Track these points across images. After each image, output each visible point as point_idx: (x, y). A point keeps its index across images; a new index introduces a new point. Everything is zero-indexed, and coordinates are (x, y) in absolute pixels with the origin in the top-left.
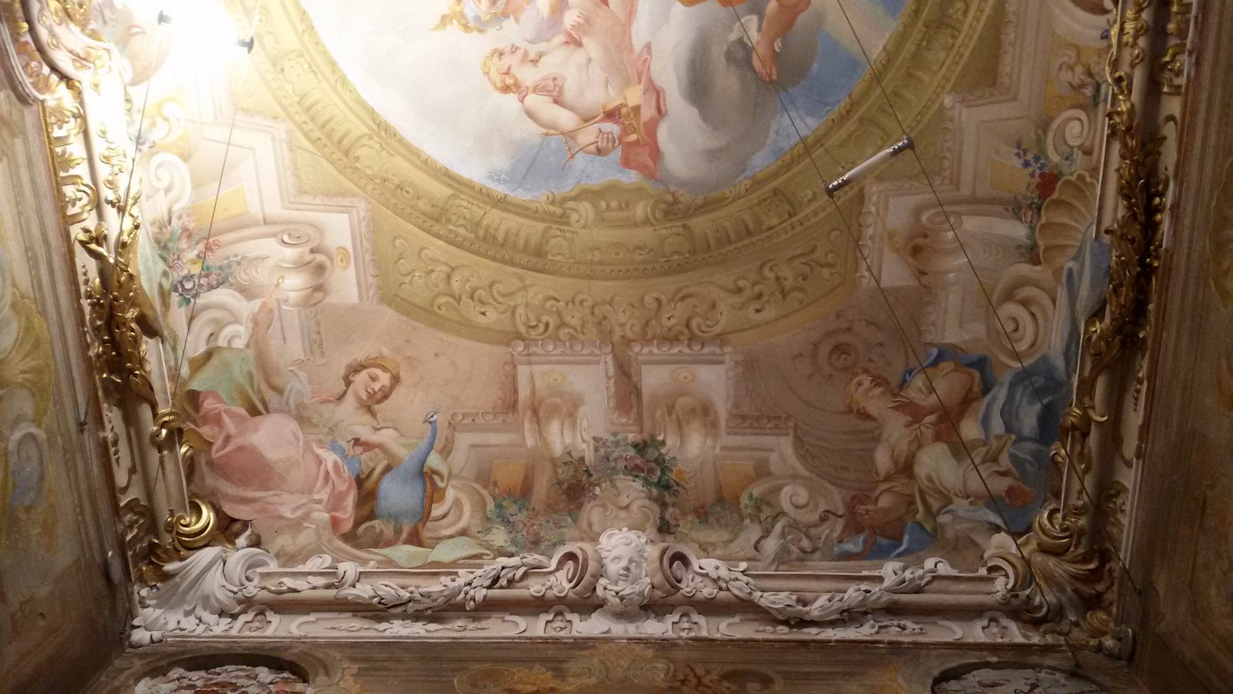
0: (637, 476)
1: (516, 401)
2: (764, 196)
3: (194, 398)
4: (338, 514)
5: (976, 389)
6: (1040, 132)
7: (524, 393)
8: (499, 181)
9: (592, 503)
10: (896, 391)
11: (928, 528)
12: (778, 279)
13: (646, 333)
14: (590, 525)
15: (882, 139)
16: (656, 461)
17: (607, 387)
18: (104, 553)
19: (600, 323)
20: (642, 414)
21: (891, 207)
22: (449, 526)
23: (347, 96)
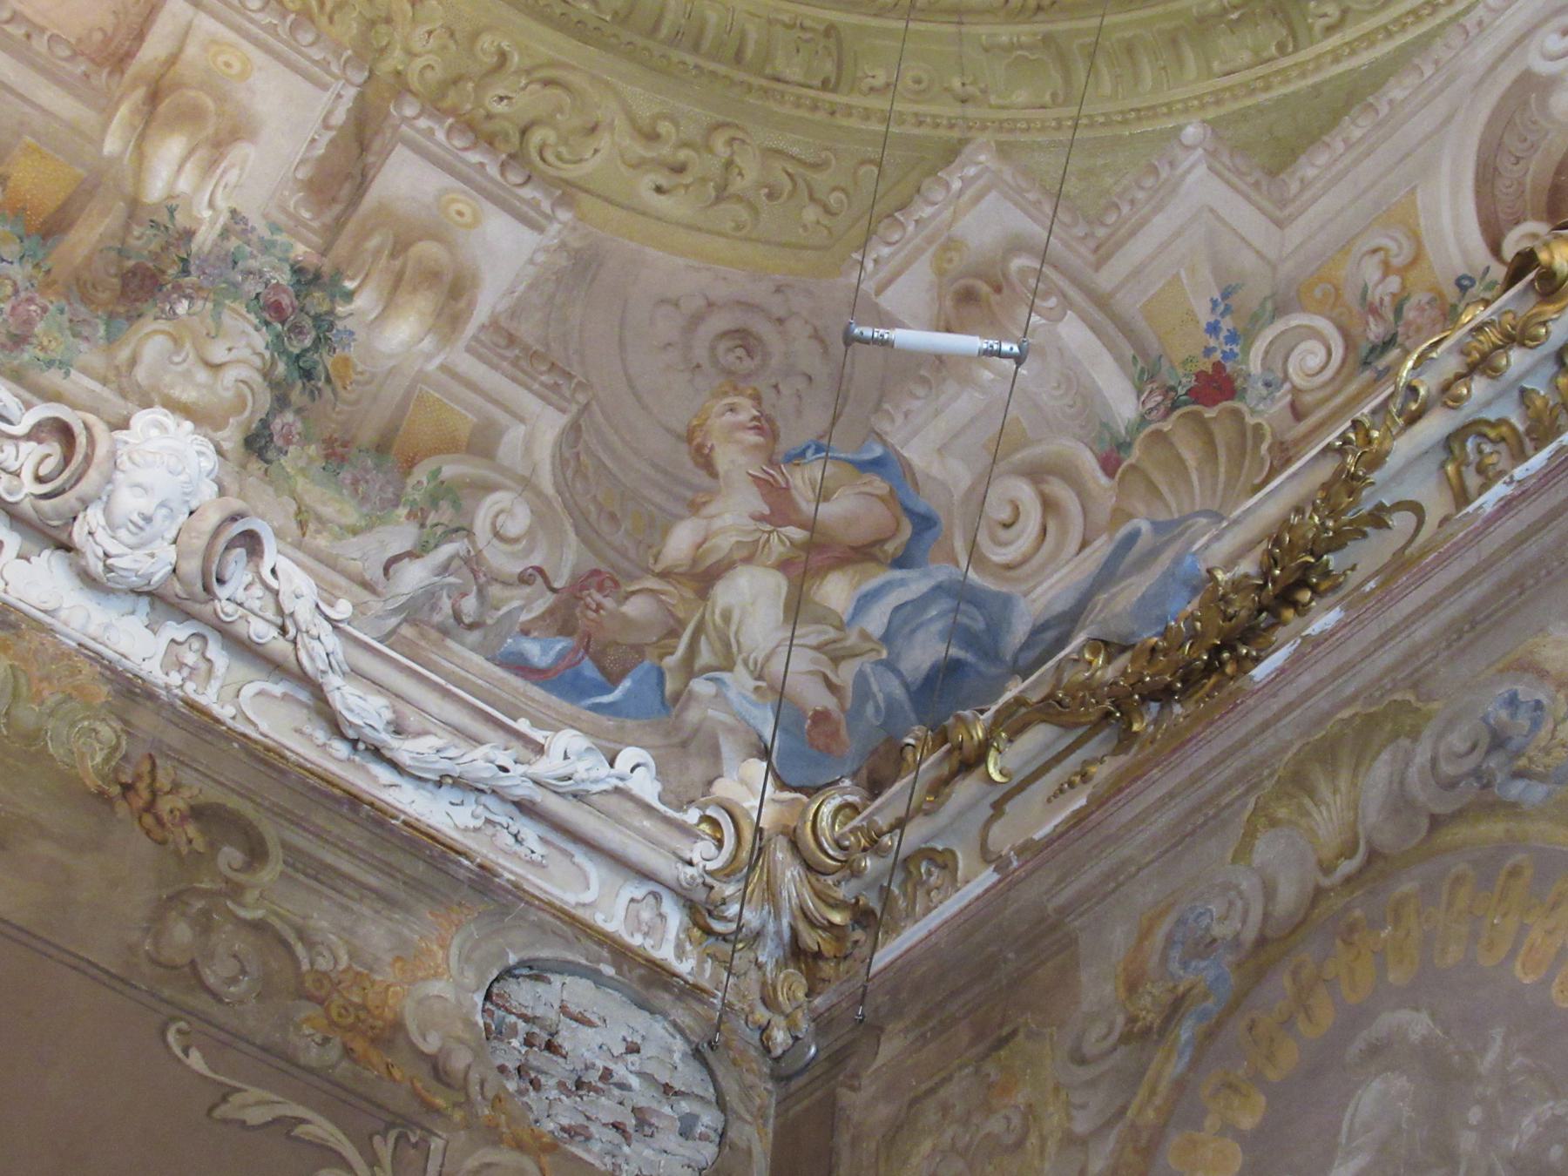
0: (267, 324)
1: (129, 55)
2: (808, 23)
6: (1269, 306)
7: (154, 49)
9: (162, 325)
10: (780, 458)
11: (670, 687)
12: (729, 164)
13: (444, 96)
14: (133, 362)
15: (1054, 95)
16: (317, 318)
17: (313, 140)
19: (372, 23)
20: (344, 224)
21: (984, 204)
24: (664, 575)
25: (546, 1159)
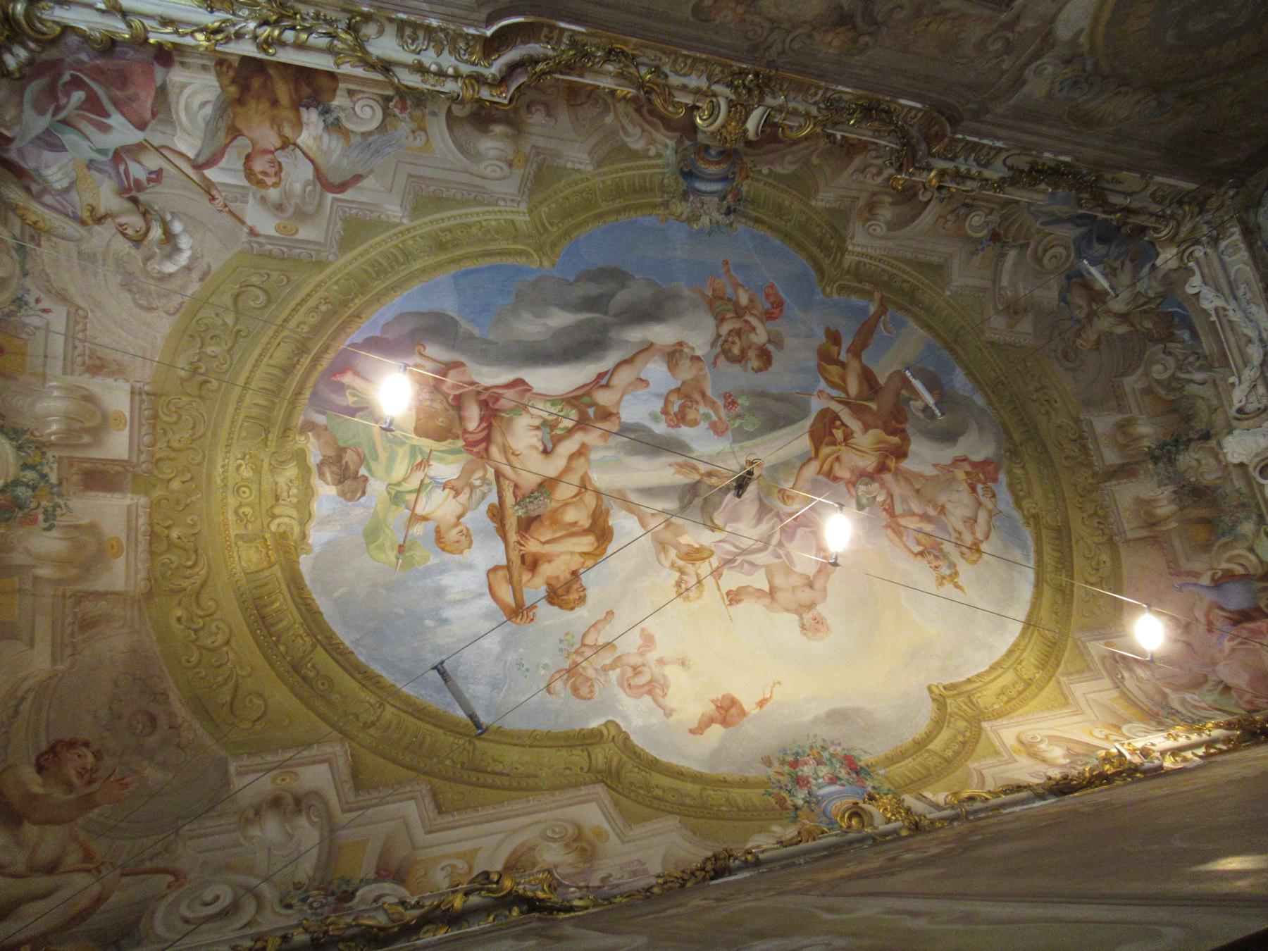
5: (1080, 281)
7: (1144, 533)
8: (1028, 555)
11: (1159, 301)
12: (1036, 391)
22: (1250, 561)
23: (1023, 644)
24: (1133, 325)
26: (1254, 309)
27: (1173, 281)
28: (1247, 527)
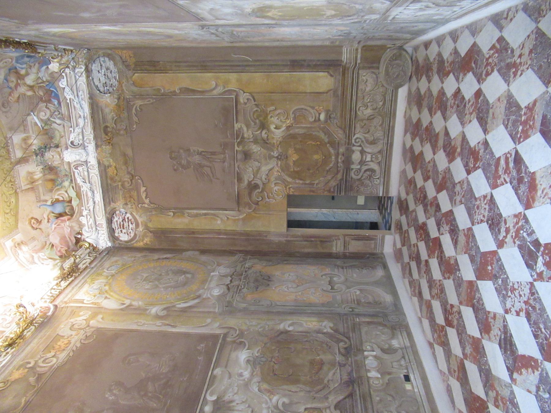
1: (31, 188)
3: (61, 257)
4: (66, 220)
7: (29, 186)
9: (53, 164)
11: (48, 83)
14: (59, 164)
18: (105, 256)
22: (65, 195)
25: (121, 83)
26: (83, 102)
27: (55, 78)
28: (66, 184)
